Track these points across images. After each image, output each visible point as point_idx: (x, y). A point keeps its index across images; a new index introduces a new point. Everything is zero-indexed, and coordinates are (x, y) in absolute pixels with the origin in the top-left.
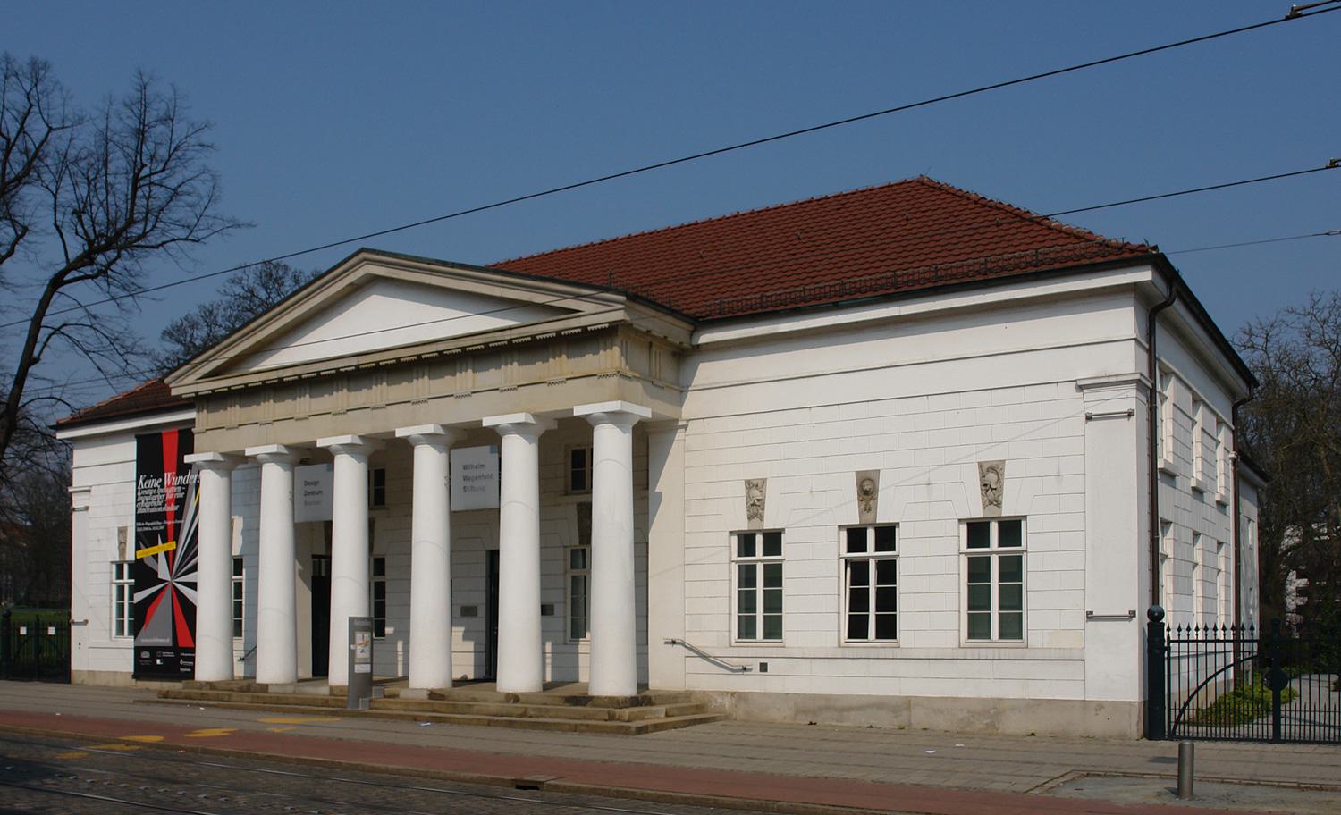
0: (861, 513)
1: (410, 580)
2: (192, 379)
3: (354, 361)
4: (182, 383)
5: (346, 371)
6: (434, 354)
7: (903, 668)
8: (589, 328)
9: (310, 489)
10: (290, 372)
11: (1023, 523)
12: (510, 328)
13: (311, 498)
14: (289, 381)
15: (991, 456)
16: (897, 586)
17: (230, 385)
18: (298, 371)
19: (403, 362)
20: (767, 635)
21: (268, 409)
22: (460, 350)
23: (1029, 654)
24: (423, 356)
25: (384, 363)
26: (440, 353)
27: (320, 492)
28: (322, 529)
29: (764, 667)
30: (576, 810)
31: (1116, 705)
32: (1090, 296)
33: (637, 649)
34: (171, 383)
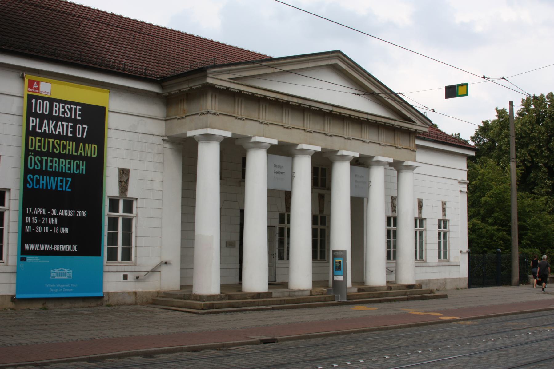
0: (419, 215)
1: (194, 223)
2: (226, 77)
3: (331, 108)
4: (217, 77)
5: (325, 111)
6: (318, 109)
7: (429, 269)
8: (243, 92)
9: (278, 170)
10: (295, 100)
11: (7, 195)
12: (392, 120)
13: (278, 176)
14: (314, 110)
15: (444, 200)
16: (386, 239)
17: (417, 129)
18: (300, 101)
19: (352, 118)
20: (123, 259)
21: (270, 116)
22: (319, 109)
23: (427, 264)
24: (352, 116)
25: (344, 115)
26: (368, 119)
27: (284, 173)
28: (284, 196)
29: (125, 277)
30: (110, 361)
31: (465, 278)
32: (9, 68)
33: (221, 266)
34: (211, 73)
